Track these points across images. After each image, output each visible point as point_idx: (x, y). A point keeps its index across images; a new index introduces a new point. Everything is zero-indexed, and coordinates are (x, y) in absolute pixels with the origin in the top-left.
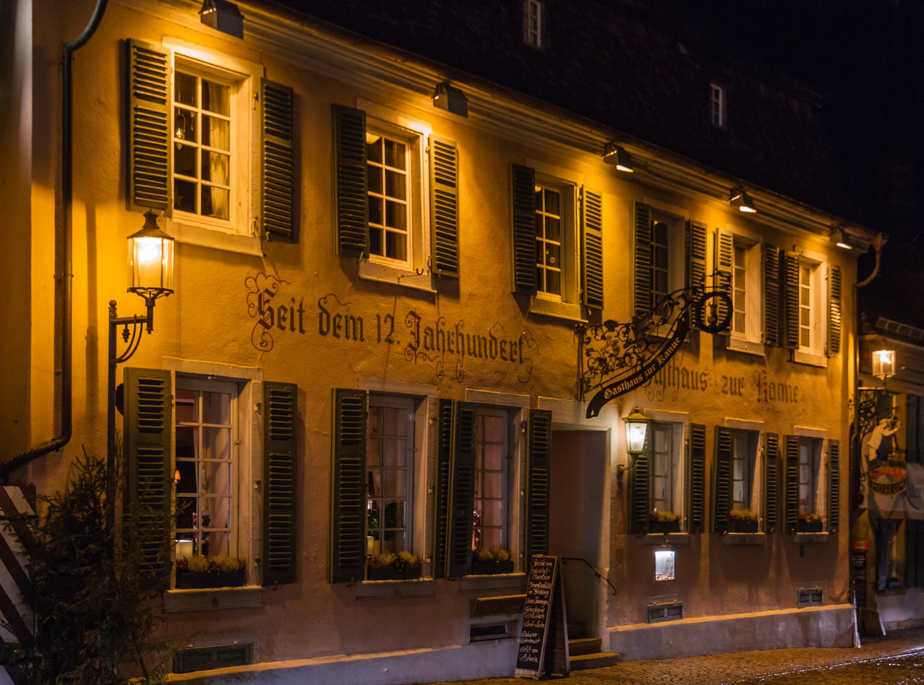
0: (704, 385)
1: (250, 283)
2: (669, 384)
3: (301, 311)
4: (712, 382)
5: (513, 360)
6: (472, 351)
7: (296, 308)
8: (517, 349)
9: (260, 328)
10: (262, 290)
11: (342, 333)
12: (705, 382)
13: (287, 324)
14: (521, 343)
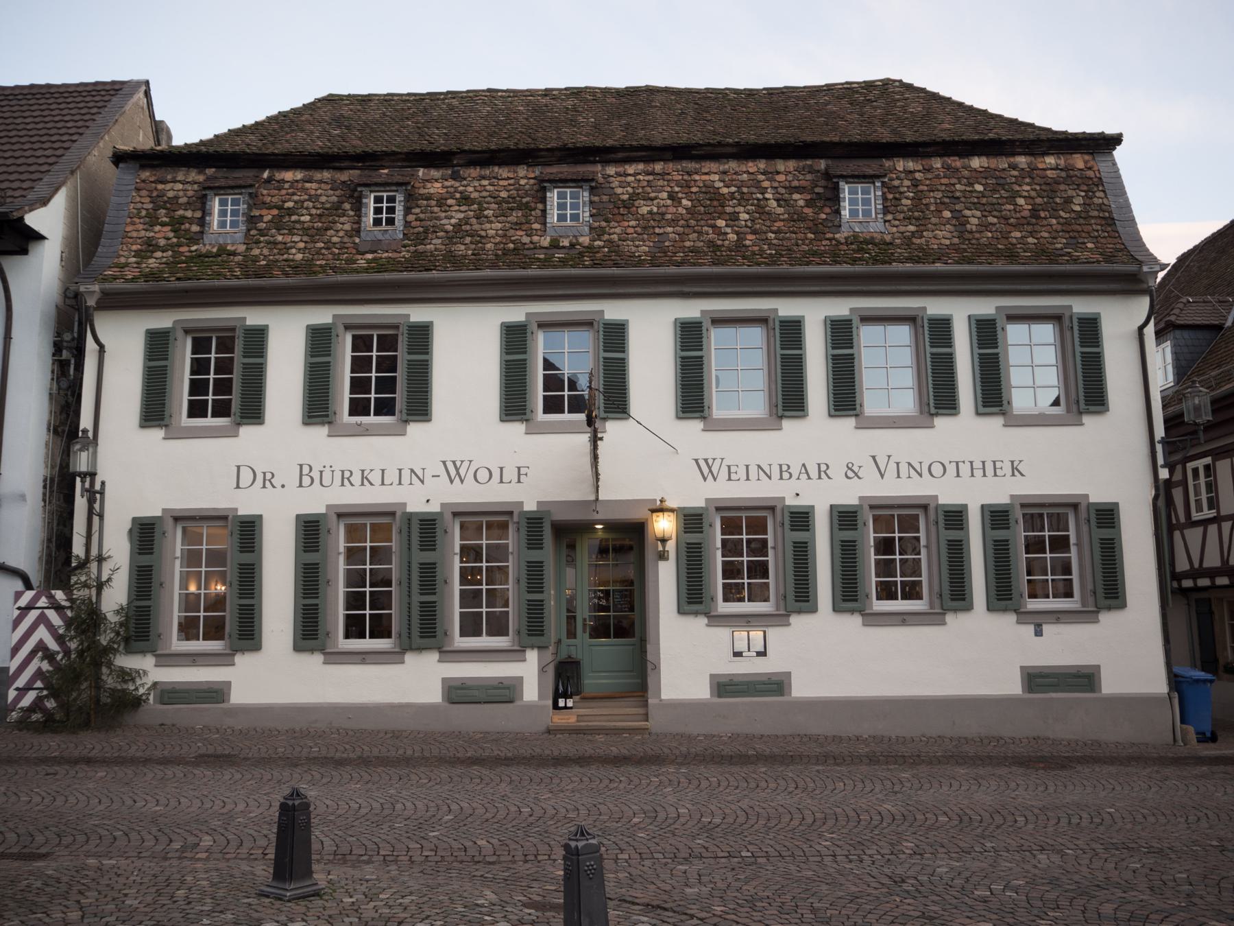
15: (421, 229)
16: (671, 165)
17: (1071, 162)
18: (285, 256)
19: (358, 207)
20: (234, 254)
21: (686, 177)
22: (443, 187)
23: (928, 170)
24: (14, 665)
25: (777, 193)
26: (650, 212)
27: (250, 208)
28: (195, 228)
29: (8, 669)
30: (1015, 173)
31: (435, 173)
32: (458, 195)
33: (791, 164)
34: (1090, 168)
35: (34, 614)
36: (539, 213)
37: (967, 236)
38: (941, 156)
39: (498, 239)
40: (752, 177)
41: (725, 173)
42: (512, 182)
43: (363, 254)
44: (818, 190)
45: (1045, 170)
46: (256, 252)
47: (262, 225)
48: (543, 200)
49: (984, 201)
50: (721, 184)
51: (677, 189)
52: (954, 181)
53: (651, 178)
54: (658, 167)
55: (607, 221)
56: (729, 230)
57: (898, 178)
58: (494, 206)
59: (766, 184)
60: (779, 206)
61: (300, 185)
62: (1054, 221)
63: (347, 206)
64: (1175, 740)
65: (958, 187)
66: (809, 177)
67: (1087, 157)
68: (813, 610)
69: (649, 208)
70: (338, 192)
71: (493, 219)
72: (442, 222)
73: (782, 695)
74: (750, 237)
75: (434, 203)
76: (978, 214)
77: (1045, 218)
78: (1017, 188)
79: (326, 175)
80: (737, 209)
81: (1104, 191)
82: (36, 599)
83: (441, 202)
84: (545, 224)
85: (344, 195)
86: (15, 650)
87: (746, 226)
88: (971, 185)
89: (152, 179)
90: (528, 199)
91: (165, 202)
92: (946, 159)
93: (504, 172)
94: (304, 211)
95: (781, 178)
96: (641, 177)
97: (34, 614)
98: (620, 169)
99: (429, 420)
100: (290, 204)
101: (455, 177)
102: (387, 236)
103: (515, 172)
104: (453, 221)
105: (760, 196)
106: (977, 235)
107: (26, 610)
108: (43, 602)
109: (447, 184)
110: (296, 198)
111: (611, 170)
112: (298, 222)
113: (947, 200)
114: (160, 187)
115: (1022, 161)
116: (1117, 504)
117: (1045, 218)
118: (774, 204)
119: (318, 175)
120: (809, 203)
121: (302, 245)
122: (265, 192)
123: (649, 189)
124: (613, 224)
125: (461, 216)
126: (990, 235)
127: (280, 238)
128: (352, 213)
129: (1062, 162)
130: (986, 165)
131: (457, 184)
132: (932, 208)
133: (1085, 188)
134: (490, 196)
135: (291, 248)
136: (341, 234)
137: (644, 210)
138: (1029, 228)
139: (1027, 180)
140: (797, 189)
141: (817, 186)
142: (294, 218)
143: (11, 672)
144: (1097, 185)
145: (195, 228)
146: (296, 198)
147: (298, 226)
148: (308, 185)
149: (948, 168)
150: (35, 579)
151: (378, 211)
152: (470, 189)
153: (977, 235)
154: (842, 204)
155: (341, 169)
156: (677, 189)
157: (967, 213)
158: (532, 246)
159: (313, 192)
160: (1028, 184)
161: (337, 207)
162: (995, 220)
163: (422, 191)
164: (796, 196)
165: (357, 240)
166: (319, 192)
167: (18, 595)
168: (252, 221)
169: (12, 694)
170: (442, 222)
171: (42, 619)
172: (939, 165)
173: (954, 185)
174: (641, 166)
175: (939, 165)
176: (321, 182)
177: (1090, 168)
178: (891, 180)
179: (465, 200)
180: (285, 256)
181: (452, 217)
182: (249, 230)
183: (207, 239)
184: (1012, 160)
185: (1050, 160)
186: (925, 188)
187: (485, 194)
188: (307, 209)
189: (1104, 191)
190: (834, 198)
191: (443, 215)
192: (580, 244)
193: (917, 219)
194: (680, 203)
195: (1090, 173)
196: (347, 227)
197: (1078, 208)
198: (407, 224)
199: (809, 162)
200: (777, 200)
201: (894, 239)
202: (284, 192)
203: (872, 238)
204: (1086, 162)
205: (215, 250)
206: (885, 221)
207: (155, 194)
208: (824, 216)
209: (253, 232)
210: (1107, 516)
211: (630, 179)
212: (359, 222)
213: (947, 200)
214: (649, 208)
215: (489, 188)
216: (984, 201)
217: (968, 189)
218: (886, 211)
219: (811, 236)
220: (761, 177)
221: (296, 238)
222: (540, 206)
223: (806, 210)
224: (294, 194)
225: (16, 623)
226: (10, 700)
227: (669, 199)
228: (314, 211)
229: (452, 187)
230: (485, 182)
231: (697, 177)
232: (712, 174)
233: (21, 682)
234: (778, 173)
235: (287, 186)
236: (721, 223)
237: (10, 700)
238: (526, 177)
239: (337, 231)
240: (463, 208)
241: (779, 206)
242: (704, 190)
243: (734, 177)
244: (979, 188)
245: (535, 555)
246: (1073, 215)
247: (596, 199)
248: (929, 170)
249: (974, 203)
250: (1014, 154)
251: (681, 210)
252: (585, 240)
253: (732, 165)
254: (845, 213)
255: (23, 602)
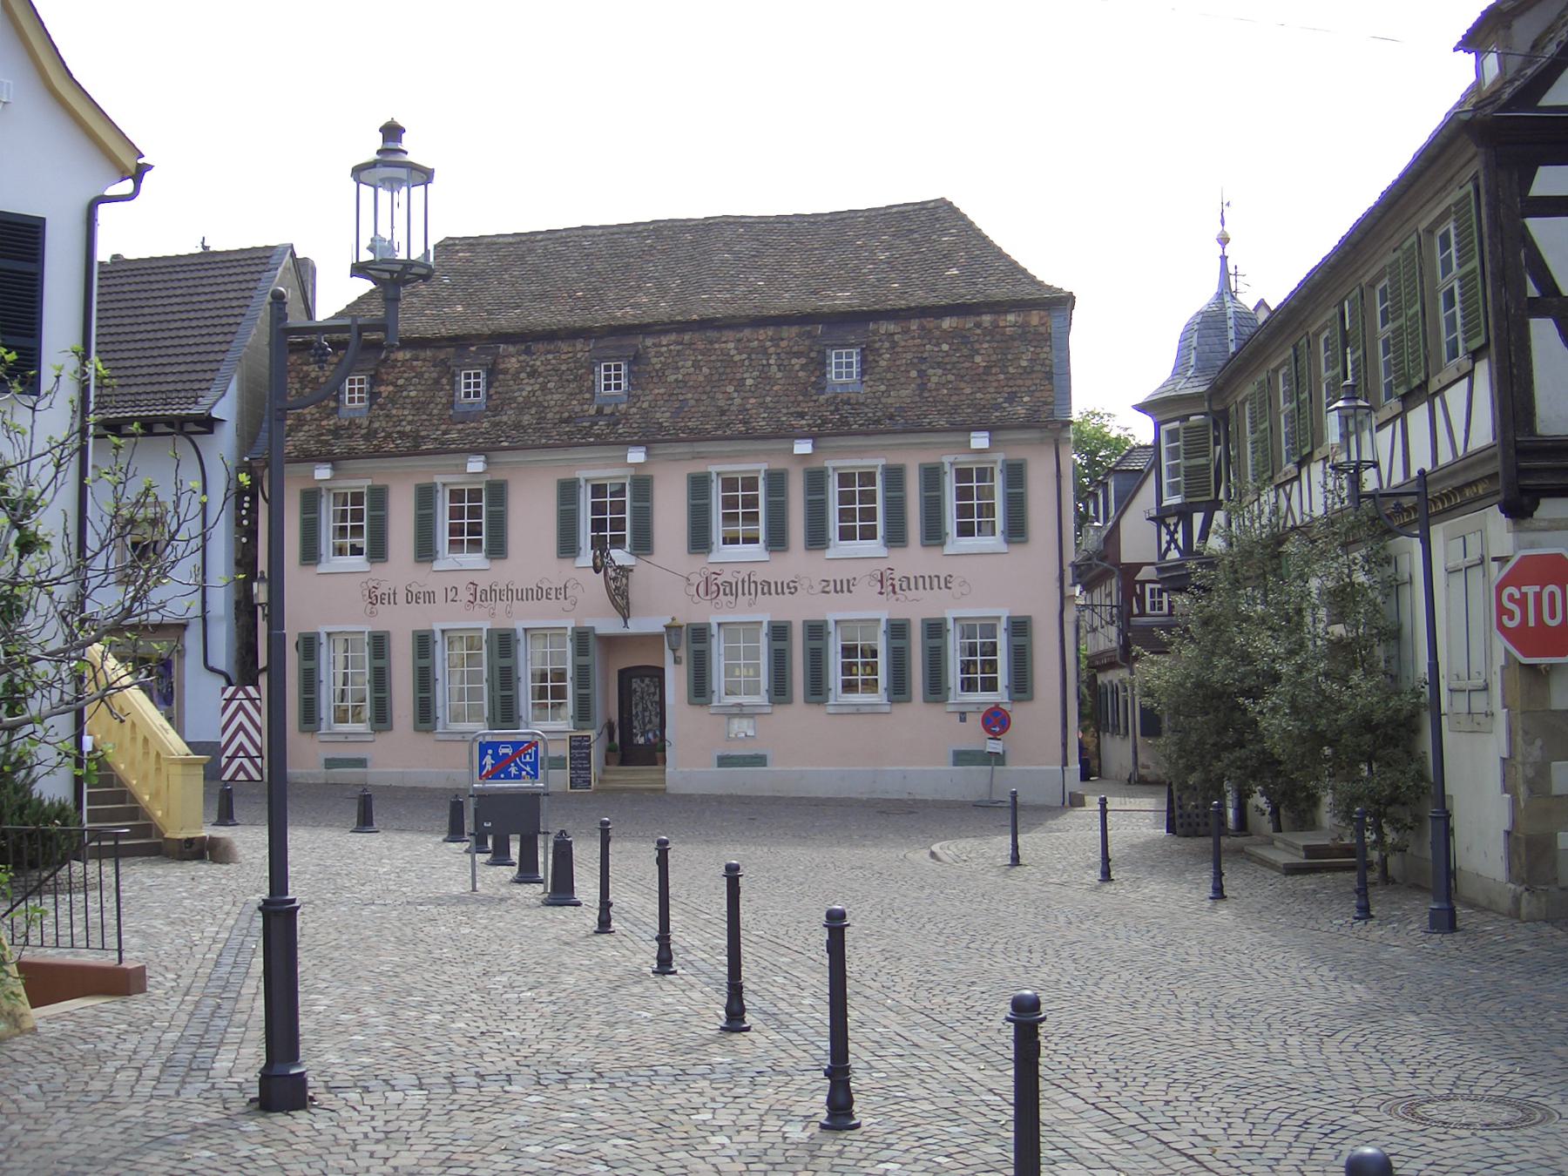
0: (793, 590)
1: (364, 585)
2: (743, 594)
3: (395, 594)
4: (806, 585)
5: (557, 598)
6: (520, 597)
7: (392, 592)
8: (563, 591)
9: (370, 606)
10: (371, 586)
11: (421, 601)
12: (796, 588)
13: (386, 601)
14: (565, 587)
15: (499, 402)
16: (697, 335)
17: (1027, 319)
18: (398, 428)
19: (453, 383)
20: (359, 427)
21: (708, 346)
22: (519, 362)
23: (906, 331)
24: (224, 741)
25: (779, 358)
26: (676, 380)
27: (372, 386)
28: (332, 404)
29: (220, 743)
30: (979, 331)
31: (511, 349)
32: (528, 369)
33: (795, 330)
34: (1043, 325)
35: (235, 704)
36: (590, 383)
37: (926, 395)
38: (919, 318)
39: (557, 409)
40: (762, 344)
41: (739, 340)
42: (570, 355)
43: (455, 424)
44: (813, 355)
45: (1006, 327)
46: (376, 425)
47: (380, 400)
48: (593, 372)
49: (947, 360)
50: (736, 352)
51: (700, 358)
52: (926, 341)
53: (680, 347)
54: (687, 337)
55: (643, 390)
56: (736, 395)
57: (880, 340)
58: (556, 378)
59: (772, 350)
60: (779, 370)
61: (409, 364)
62: (1002, 377)
63: (444, 381)
64: (1063, 803)
65: (928, 347)
66: (807, 343)
67: (1042, 313)
68: (790, 702)
69: (675, 376)
70: (438, 369)
71: (554, 391)
72: (516, 394)
73: (765, 765)
74: (752, 401)
75: (509, 377)
76: (940, 372)
77: (996, 374)
78: (977, 346)
79: (429, 353)
80: (745, 376)
81: (1050, 346)
82: (235, 693)
83: (516, 377)
84: (594, 394)
85: (441, 372)
86: (224, 729)
87: (750, 391)
88: (938, 345)
89: (299, 362)
90: (583, 371)
91: (310, 382)
92: (923, 320)
93: (564, 347)
94: (412, 388)
95: (783, 344)
96: (672, 347)
97: (235, 704)
98: (657, 341)
99: (506, 558)
100: (401, 382)
101: (528, 352)
102: (473, 409)
103: (574, 345)
104: (524, 394)
105: (765, 362)
106: (934, 394)
107: (229, 701)
108: (241, 695)
109: (521, 358)
110: (406, 375)
111: (649, 342)
112: (408, 397)
113: (915, 361)
114: (305, 368)
115: (987, 319)
116: (1029, 617)
117: (996, 374)
118: (774, 368)
119: (422, 355)
120: (803, 367)
121: (410, 418)
122: (383, 370)
123: (677, 359)
124: (648, 392)
125: (529, 389)
126: (945, 391)
127: (394, 412)
128: (448, 387)
129: (1020, 320)
130: (955, 325)
131: (529, 359)
132: (903, 369)
133: (1035, 344)
134: (553, 369)
135: (403, 420)
136: (440, 407)
137: (672, 378)
138: (980, 384)
139: (988, 338)
140: (798, 355)
141: (812, 350)
142: (405, 393)
143: (222, 745)
144: (1046, 340)
145: (332, 404)
146: (406, 375)
147: (408, 401)
148: (415, 363)
149: (922, 328)
150: (234, 681)
151: (468, 386)
152: (538, 363)
153: (934, 394)
154: (828, 369)
155: (440, 348)
156: (700, 358)
157: (930, 372)
158: (581, 414)
159: (419, 370)
160: (987, 342)
161: (437, 381)
162: (953, 378)
163: (501, 366)
164: (794, 361)
165: (451, 412)
166: (424, 369)
167: (224, 690)
168: (373, 396)
169: (224, 761)
170: (516, 394)
171: (241, 707)
172: (914, 327)
173: (924, 345)
174: (673, 337)
175: (915, 327)
176: (424, 360)
177: (1043, 325)
178: (875, 342)
179: (533, 373)
180: (398, 428)
181: (523, 390)
182: (371, 405)
183: (343, 412)
184: (978, 319)
185: (1011, 318)
186: (900, 350)
187: (549, 367)
188: (414, 385)
189: (1050, 346)
190: (822, 364)
191: (516, 387)
192: (619, 411)
193: (888, 380)
194: (701, 370)
195: (1042, 329)
196: (444, 400)
197: (1024, 364)
198: (489, 397)
199: (808, 328)
200: (779, 366)
201: (866, 398)
202: (397, 370)
203: (849, 398)
204: (1041, 318)
205: (347, 423)
206: (863, 382)
207: (301, 375)
208: (813, 379)
209: (375, 407)
210: (1020, 628)
211: (664, 349)
212: (453, 395)
213: (915, 361)
214: (675, 376)
215: (553, 362)
216: (947, 360)
217: (936, 349)
218: (863, 373)
219: (800, 398)
220: (768, 344)
221: (406, 412)
222: (591, 377)
223: (801, 374)
224: (405, 372)
225: (224, 709)
226: (223, 764)
227: (693, 366)
228: (419, 387)
229: (524, 361)
230: (550, 356)
231: (717, 346)
232: (728, 343)
233: (229, 753)
234: (782, 339)
235: (399, 364)
236: (730, 389)
237: (223, 764)
238: (581, 351)
239: (437, 404)
240: (532, 381)
241: (779, 370)
242: (720, 358)
243: (747, 344)
244: (945, 347)
245: (583, 660)
246: (1020, 371)
247: (636, 369)
248: (906, 333)
249: (939, 363)
250: (980, 314)
251: (701, 378)
252: (623, 407)
253: (747, 332)
254: (832, 375)
255: (228, 694)
